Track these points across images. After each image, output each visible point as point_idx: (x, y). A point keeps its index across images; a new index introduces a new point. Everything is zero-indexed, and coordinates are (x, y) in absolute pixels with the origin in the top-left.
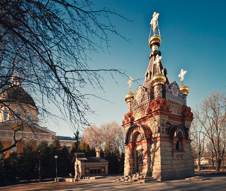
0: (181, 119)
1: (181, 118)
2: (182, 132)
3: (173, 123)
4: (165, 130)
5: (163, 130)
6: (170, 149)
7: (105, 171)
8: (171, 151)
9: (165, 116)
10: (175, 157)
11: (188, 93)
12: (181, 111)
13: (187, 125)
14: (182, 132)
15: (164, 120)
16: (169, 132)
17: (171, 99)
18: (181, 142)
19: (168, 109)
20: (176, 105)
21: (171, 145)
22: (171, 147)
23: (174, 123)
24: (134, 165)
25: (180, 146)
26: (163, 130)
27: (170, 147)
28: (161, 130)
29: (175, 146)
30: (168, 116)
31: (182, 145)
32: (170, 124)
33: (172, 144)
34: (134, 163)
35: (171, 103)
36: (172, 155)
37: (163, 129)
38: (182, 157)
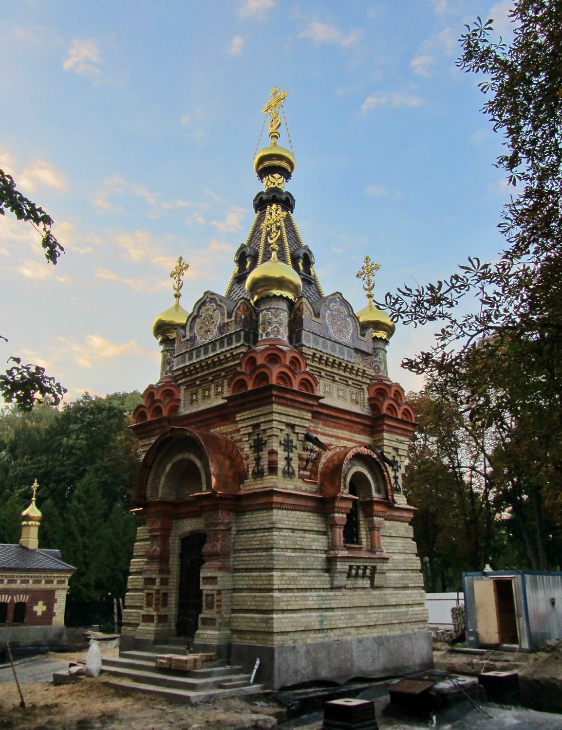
0: (364, 425)
1: (367, 422)
2: (369, 477)
3: (332, 436)
4: (295, 464)
5: (289, 464)
6: (321, 542)
7: (49, 615)
8: (326, 552)
9: (297, 411)
10: (341, 580)
11: (390, 335)
12: (367, 396)
13: (390, 450)
14: (369, 477)
15: (292, 426)
16: (314, 472)
17: (328, 349)
18: (369, 515)
19: (307, 384)
20: (345, 371)
21: (321, 527)
22: (325, 533)
23: (337, 437)
24: (165, 604)
25: (363, 534)
26: (289, 464)
27: (318, 532)
28: (281, 464)
29: (339, 532)
30: (309, 411)
31: (372, 528)
32: (316, 442)
33: (331, 524)
34: (165, 595)
35: (326, 365)
36: (327, 570)
37: (288, 460)
38: (372, 579)
